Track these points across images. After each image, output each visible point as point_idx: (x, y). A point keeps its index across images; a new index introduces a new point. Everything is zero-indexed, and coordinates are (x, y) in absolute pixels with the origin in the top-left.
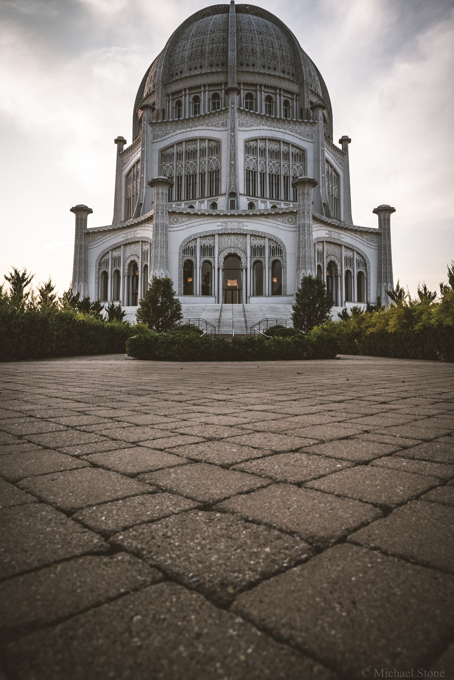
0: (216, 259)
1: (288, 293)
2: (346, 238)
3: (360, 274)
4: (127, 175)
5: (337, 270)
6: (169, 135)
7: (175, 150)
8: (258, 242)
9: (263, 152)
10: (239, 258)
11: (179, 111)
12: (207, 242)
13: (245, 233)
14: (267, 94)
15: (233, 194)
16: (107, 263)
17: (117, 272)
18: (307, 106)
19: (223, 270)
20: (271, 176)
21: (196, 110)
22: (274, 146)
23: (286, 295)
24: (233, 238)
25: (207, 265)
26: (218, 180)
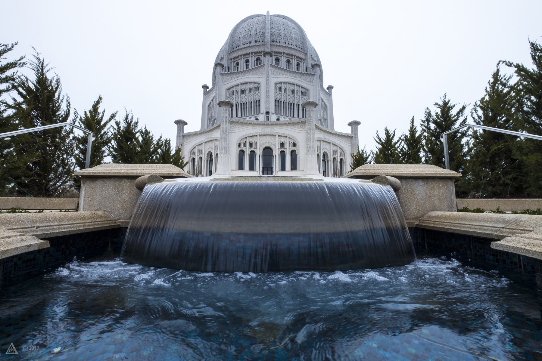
1: (301, 169)
2: (332, 139)
3: (341, 160)
4: (209, 106)
5: (328, 157)
7: (234, 89)
8: (283, 140)
9: (284, 90)
10: (271, 149)
11: (238, 68)
15: (268, 113)
16: (195, 153)
17: (201, 158)
18: (310, 66)
20: (289, 104)
21: (247, 66)
22: (291, 87)
23: (299, 170)
24: (268, 137)
25: (253, 153)
26: (259, 105)
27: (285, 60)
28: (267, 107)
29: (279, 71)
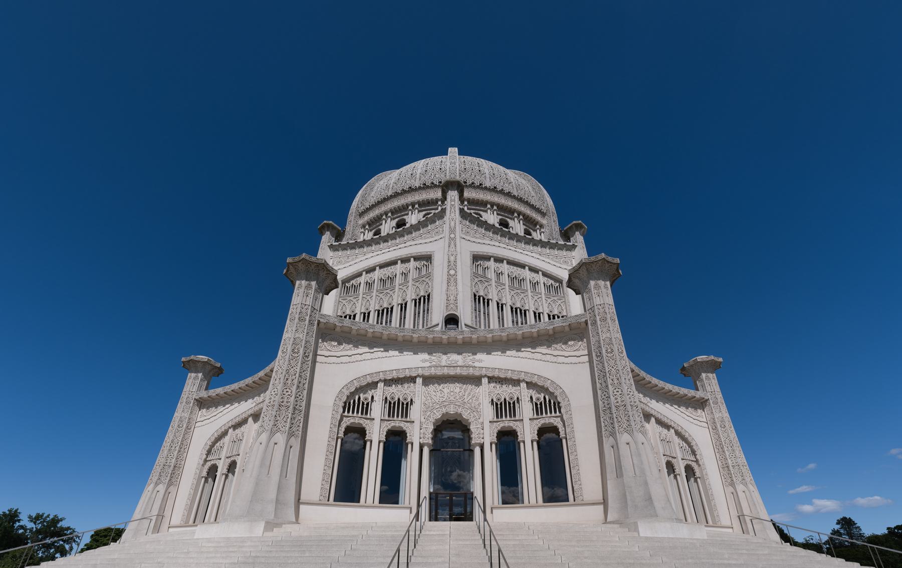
0: (417, 425)
6: (357, 260)
8: (506, 392)
10: (465, 429)
12: (397, 392)
13: (477, 373)
14: (500, 217)
19: (431, 451)
22: (517, 271)
28: (450, 301)
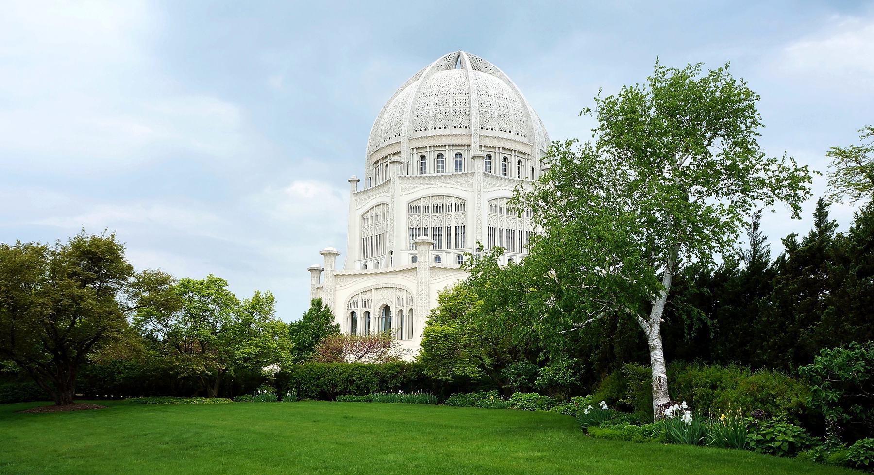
17: (368, 314)
27: (501, 159)
29: (494, 181)
